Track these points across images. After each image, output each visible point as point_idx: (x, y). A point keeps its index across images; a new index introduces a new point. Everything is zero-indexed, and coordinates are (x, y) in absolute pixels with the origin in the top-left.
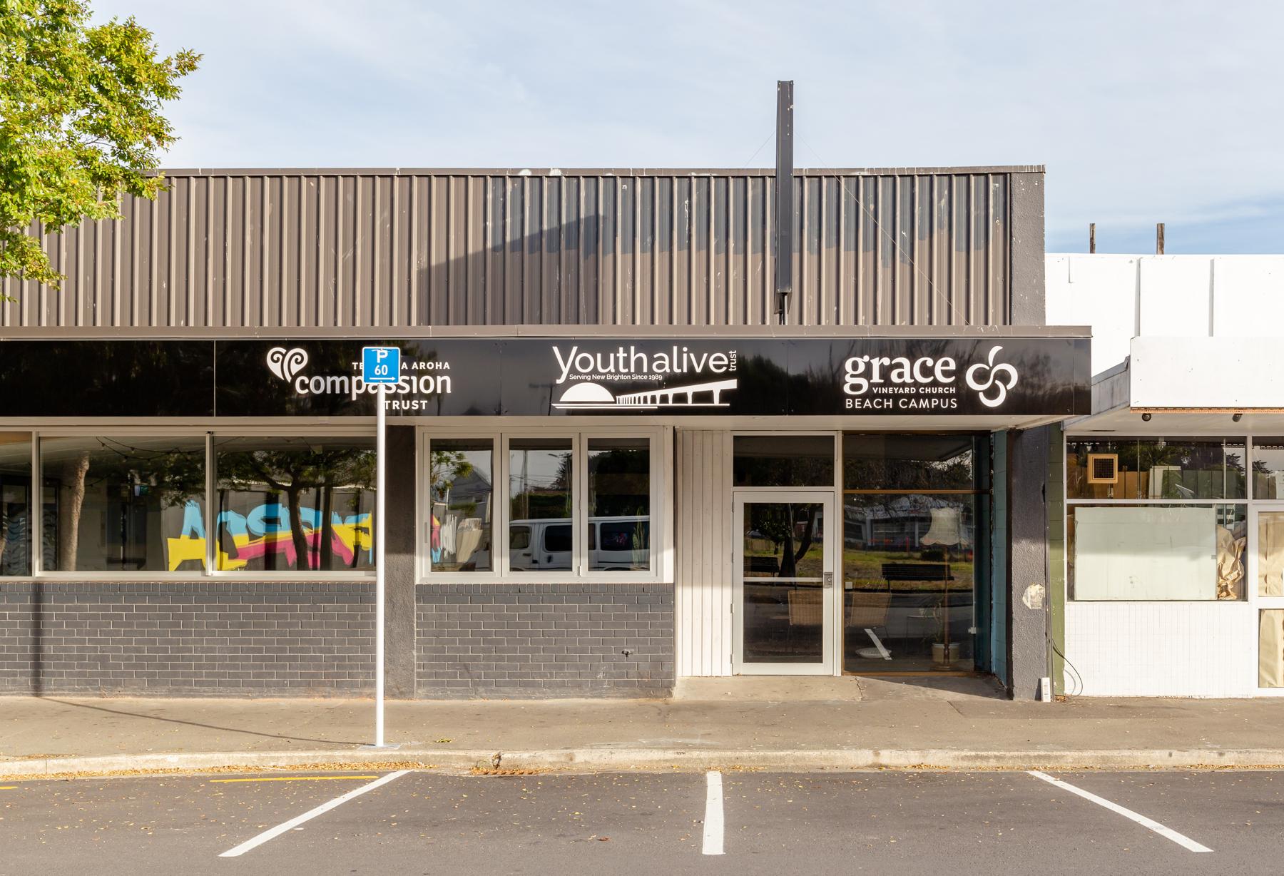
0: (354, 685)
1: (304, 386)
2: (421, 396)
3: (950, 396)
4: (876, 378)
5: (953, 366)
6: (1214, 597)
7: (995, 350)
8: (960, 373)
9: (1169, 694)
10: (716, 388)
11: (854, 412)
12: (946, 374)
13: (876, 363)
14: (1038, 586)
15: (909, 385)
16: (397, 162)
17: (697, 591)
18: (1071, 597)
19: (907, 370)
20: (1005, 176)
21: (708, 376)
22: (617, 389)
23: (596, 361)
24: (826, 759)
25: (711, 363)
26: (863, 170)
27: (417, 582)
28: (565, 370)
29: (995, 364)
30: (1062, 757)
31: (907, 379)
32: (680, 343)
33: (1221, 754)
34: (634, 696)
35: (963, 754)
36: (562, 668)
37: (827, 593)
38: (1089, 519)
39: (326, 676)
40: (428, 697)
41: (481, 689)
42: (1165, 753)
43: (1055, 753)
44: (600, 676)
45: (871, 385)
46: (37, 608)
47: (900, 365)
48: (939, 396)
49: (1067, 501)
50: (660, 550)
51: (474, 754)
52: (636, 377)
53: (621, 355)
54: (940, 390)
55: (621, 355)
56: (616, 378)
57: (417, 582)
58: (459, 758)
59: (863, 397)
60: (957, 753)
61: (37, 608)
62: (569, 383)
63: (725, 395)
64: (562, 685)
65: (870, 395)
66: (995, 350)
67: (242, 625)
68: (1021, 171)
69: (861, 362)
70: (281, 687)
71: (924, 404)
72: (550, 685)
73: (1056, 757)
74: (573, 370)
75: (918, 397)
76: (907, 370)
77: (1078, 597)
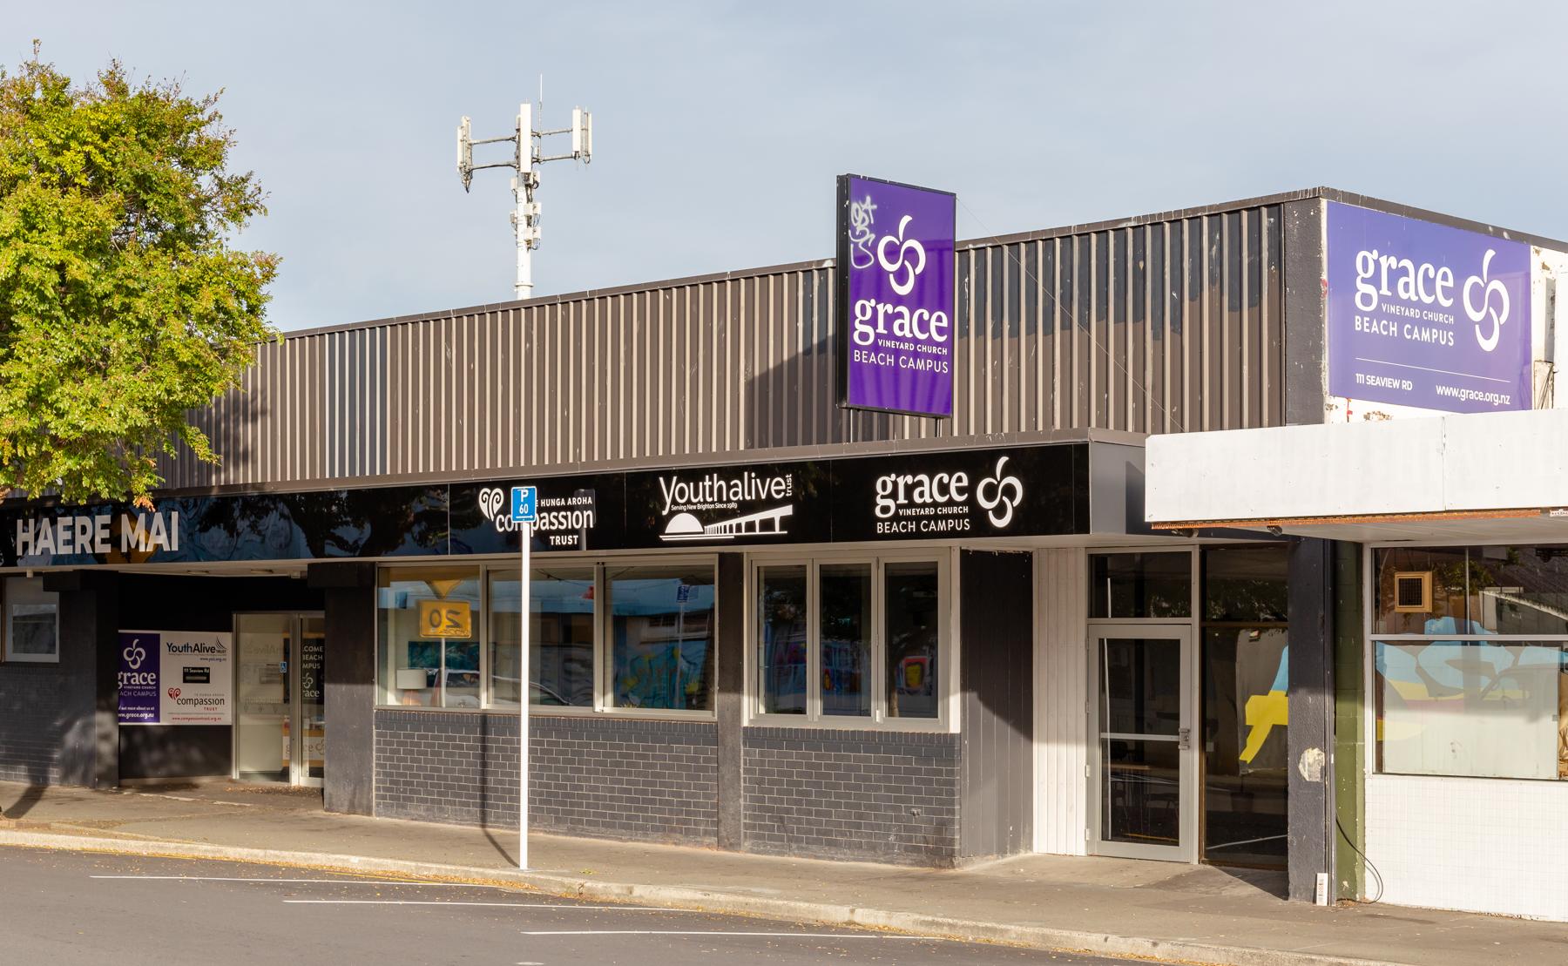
0: (696, 833)
1: (502, 524)
2: (573, 531)
3: (963, 516)
4: (902, 500)
5: (965, 483)
6: (1555, 776)
7: (1003, 460)
8: (971, 490)
9: (1493, 910)
10: (777, 514)
11: (884, 537)
12: (960, 491)
13: (901, 481)
14: (1316, 751)
15: (929, 505)
16: (728, 267)
17: (1063, 749)
18: (1380, 768)
19: (926, 489)
20: (1275, 206)
21: (771, 503)
22: (705, 517)
23: (689, 489)
24: (812, 912)
25: (773, 488)
26: (1129, 220)
27: (745, 723)
28: (669, 501)
29: (1003, 477)
30: (1007, 931)
31: (929, 500)
32: (750, 468)
33: (1155, 944)
34: (921, 864)
35: (922, 918)
36: (858, 826)
37: (1184, 756)
38: (1395, 662)
39: (678, 821)
40: (752, 851)
41: (794, 846)
42: (1099, 937)
43: (1003, 926)
44: (892, 838)
45: (899, 507)
46: (483, 740)
47: (920, 483)
48: (954, 517)
49: (1369, 637)
50: (947, 694)
51: (567, 881)
52: (719, 506)
53: (707, 483)
54: (955, 510)
55: (707, 483)
56: (704, 507)
57: (745, 723)
58: (557, 883)
59: (891, 520)
60: (917, 916)
61: (483, 740)
62: (672, 514)
63: (785, 521)
64: (859, 846)
65: (896, 518)
66: (1003, 460)
67: (618, 764)
68: (1292, 198)
69: (890, 479)
70: (644, 831)
71: (942, 526)
72: (850, 845)
73: (1002, 931)
74: (674, 502)
75: (936, 518)
76: (926, 489)
77: (1387, 770)
